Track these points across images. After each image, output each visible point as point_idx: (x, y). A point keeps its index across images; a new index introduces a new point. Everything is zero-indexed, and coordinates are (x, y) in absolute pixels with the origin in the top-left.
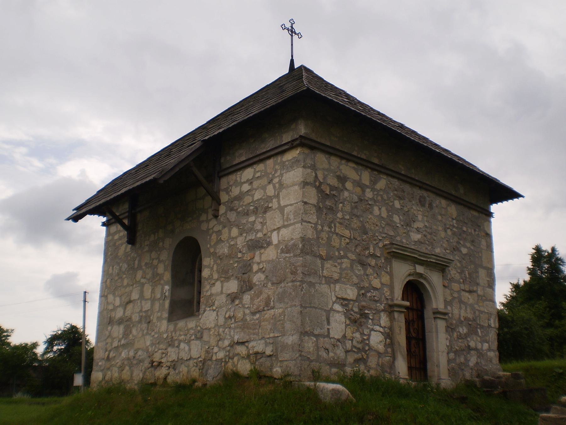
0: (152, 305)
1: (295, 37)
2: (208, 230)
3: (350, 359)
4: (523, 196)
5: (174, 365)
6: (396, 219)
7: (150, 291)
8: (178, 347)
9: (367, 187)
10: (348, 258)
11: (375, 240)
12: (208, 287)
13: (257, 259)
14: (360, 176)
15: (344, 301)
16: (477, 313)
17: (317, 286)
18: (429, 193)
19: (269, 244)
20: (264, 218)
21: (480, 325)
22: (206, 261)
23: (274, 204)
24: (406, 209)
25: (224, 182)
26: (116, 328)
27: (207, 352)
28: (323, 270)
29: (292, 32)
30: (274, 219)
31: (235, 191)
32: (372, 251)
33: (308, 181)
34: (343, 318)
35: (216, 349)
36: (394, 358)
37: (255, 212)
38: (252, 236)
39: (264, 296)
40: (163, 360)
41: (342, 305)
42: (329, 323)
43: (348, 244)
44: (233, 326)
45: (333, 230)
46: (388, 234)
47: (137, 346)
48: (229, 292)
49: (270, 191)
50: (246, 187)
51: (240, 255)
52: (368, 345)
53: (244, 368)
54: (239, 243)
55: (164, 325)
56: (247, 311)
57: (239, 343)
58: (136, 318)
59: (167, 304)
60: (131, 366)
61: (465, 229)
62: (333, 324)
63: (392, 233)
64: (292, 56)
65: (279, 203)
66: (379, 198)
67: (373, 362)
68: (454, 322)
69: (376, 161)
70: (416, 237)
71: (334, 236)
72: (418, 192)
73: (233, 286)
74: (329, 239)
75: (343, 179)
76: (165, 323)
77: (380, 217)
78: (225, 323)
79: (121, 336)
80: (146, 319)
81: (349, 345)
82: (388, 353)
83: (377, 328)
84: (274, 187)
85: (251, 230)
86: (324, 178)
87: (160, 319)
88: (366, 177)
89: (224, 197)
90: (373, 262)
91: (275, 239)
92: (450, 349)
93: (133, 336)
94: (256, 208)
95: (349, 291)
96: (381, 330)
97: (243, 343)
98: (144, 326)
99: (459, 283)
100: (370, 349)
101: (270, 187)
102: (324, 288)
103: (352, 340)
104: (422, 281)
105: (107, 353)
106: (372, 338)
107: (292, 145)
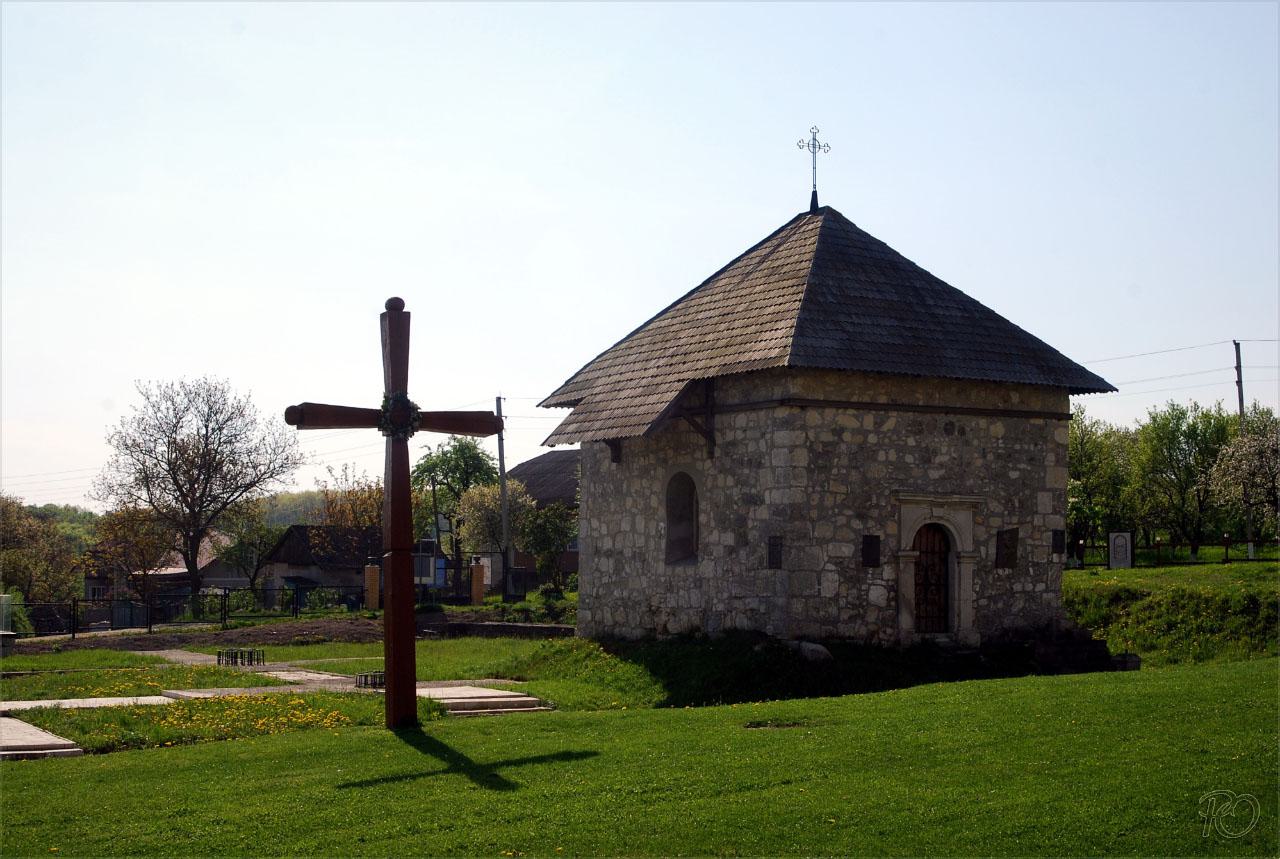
0: (646, 542)
1: (820, 154)
3: (845, 616)
4: (1117, 390)
5: (673, 613)
6: (909, 459)
7: (643, 523)
8: (678, 593)
9: (870, 432)
10: (843, 515)
11: (879, 489)
12: (706, 534)
13: (751, 514)
14: (862, 423)
15: (838, 562)
16: (1029, 548)
17: (807, 549)
18: (959, 416)
19: (763, 502)
20: (757, 473)
21: (1033, 562)
22: (703, 505)
23: (766, 461)
24: (924, 445)
25: (719, 420)
26: (604, 560)
27: (707, 602)
28: (813, 532)
29: (815, 146)
30: (766, 477)
31: (730, 436)
32: (874, 501)
33: (797, 443)
34: (836, 577)
35: (715, 601)
36: (898, 610)
38: (746, 490)
40: (662, 606)
41: (836, 564)
42: (819, 584)
43: (844, 500)
44: (731, 579)
45: (826, 488)
46: (896, 479)
47: (631, 585)
48: (726, 543)
50: (740, 435)
51: (735, 507)
52: (867, 600)
53: (742, 622)
54: (734, 494)
55: (661, 567)
56: (744, 568)
57: (736, 597)
58: (628, 553)
59: (663, 543)
60: (625, 606)
61: (1017, 447)
62: (825, 584)
63: (902, 476)
64: (815, 186)
65: (771, 463)
66: (887, 440)
67: (872, 617)
68: (990, 563)
69: (883, 399)
70: (934, 474)
71: (828, 494)
72: (942, 419)
74: (822, 499)
75: (839, 432)
76: (662, 565)
77: (888, 463)
78: (724, 575)
79: (611, 571)
80: (639, 556)
81: (842, 602)
82: (890, 606)
83: (879, 582)
84: (766, 443)
85: (745, 483)
86: (817, 437)
87: (656, 560)
88: (869, 420)
89: (719, 440)
90: (875, 513)
92: (980, 595)
93: (626, 573)
94: (750, 460)
95: (844, 549)
96: (883, 583)
98: (639, 565)
99: (1001, 515)
100: (868, 603)
102: (816, 550)
103: (846, 597)
104: (941, 522)
105: (595, 590)
106: (871, 592)
107: (783, 402)
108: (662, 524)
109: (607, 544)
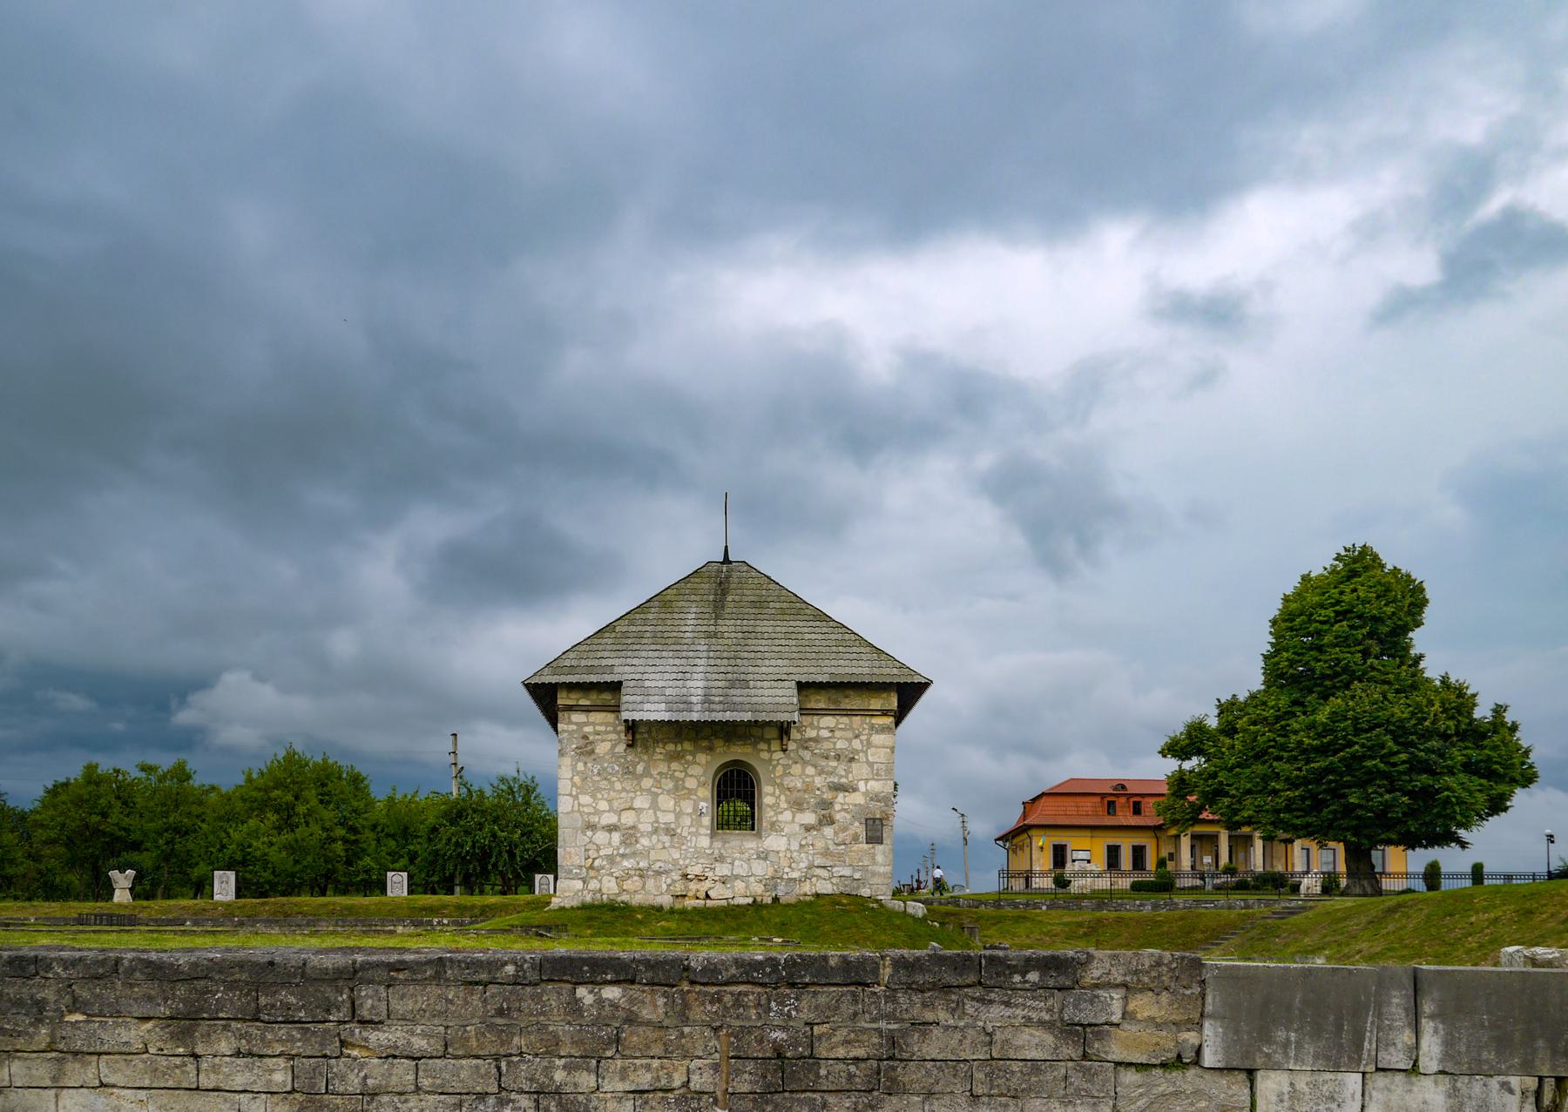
2: (770, 760)
8: (732, 864)
26: (601, 837)
30: (859, 770)
31: (812, 733)
37: (838, 757)
39: (851, 832)
49: (856, 744)
50: (825, 733)
73: (809, 818)
87: (697, 834)
91: (861, 785)
108: (703, 804)
109: (611, 819)
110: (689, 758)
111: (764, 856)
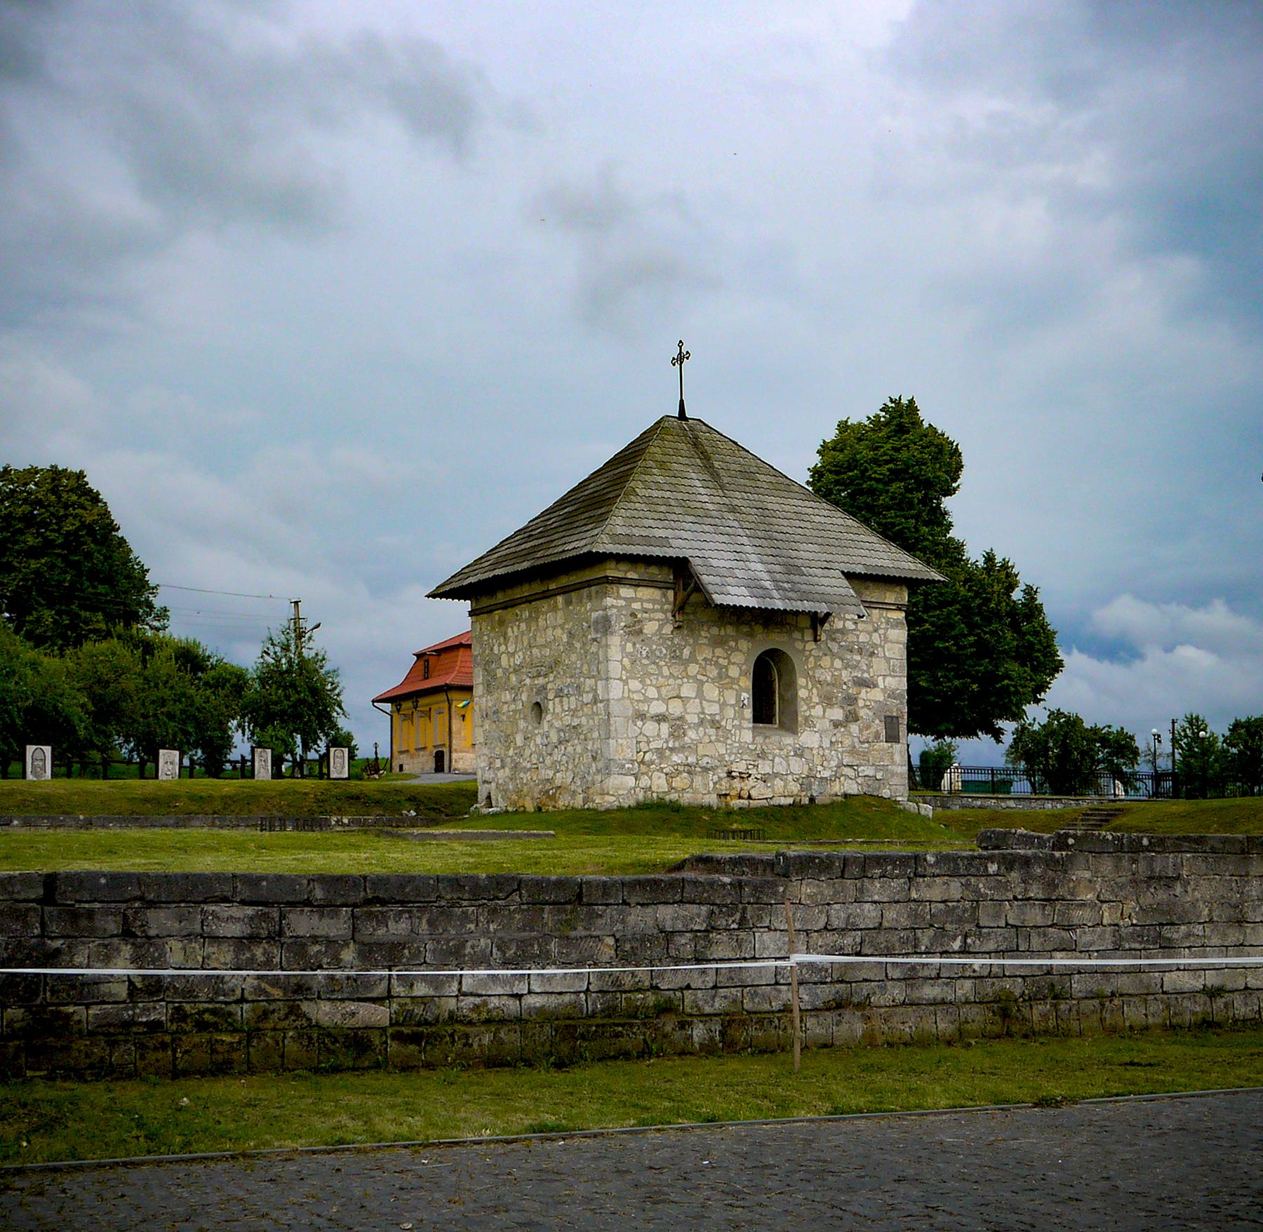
2: (804, 650)
13: (863, 695)
19: (876, 686)
22: (801, 681)
30: (879, 665)
37: (860, 651)
49: (876, 638)
50: (850, 625)
73: (837, 714)
87: (740, 727)
97: (851, 766)
101: (875, 635)
108: (745, 695)
109: (657, 708)
110: (732, 644)
111: (800, 753)
